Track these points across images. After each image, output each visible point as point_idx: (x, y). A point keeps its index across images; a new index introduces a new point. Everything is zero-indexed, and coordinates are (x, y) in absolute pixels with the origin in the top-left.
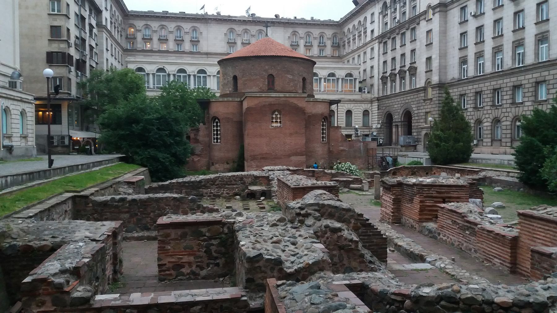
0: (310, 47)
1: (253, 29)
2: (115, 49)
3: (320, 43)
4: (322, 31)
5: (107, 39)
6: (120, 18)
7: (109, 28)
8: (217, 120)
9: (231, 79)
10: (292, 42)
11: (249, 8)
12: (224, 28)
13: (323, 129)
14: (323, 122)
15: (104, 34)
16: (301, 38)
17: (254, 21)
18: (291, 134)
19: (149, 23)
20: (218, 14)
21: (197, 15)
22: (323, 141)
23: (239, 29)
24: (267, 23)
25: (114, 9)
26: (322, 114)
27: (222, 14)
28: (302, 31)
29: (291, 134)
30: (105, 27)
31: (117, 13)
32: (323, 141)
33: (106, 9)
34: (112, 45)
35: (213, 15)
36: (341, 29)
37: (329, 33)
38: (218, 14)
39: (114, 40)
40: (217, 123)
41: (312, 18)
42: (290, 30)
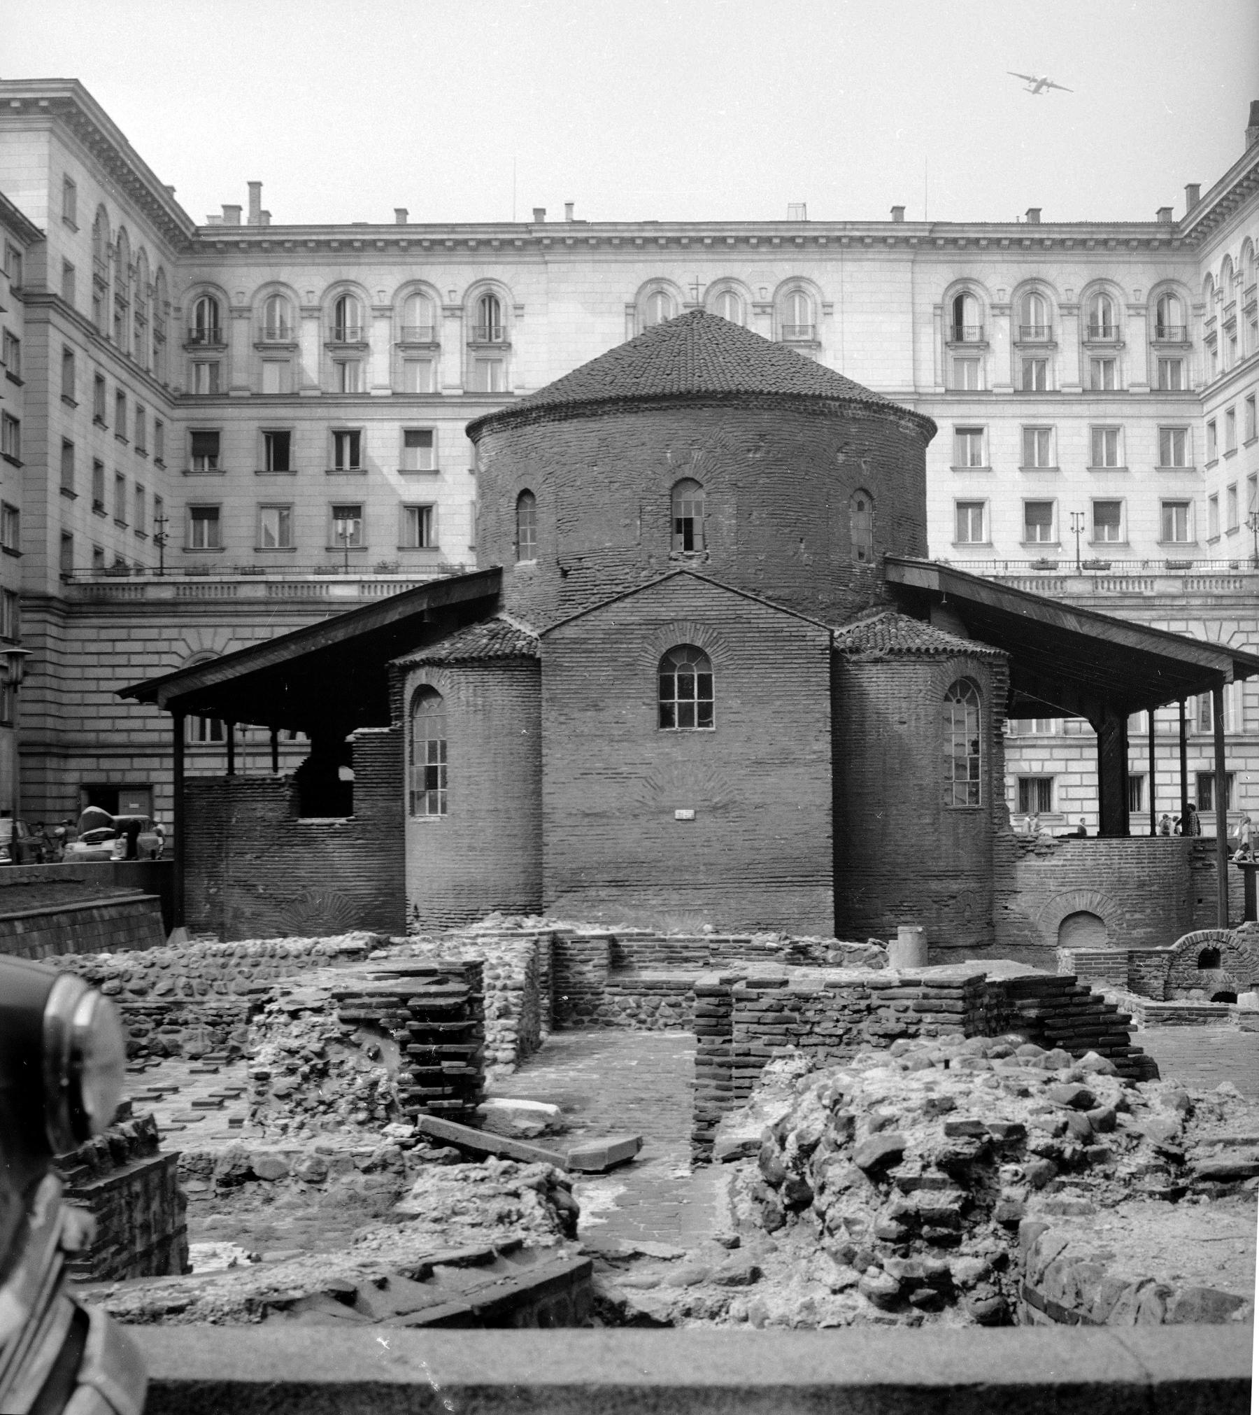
0: (1041, 353)
2: (120, 397)
4: (1099, 271)
5: (68, 355)
6: (153, 259)
7: (83, 303)
15: (51, 328)
19: (284, 274)
25: (115, 218)
30: (62, 306)
31: (136, 237)
33: (69, 221)
34: (99, 380)
36: (1198, 263)
37: (1133, 279)
39: (113, 357)
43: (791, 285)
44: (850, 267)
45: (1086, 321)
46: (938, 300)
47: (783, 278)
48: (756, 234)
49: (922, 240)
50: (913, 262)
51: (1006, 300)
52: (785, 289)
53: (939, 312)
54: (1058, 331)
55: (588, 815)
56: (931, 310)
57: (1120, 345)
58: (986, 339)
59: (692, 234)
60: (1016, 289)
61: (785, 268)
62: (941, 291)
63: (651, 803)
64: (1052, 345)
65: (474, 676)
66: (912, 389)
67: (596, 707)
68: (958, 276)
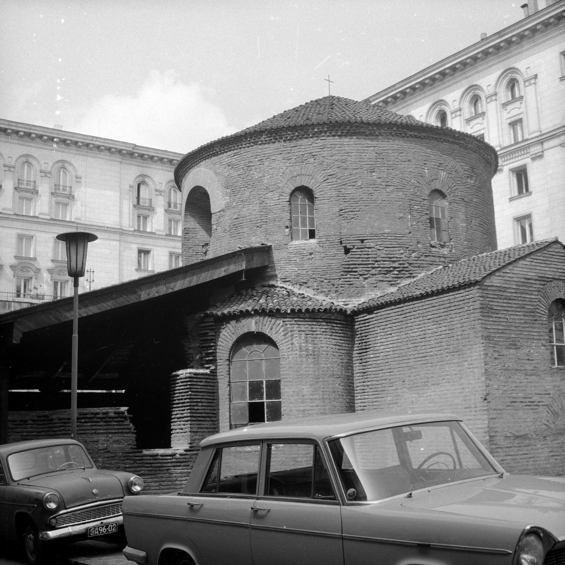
43: (60, 164)
46: (132, 183)
47: (57, 160)
48: (47, 134)
50: (121, 162)
51: (163, 188)
52: (57, 165)
53: (131, 189)
55: (517, 437)
56: (128, 188)
58: (153, 206)
59: (14, 128)
62: (133, 180)
63: (552, 426)
65: (305, 326)
66: (119, 227)
67: (514, 345)
68: (141, 173)
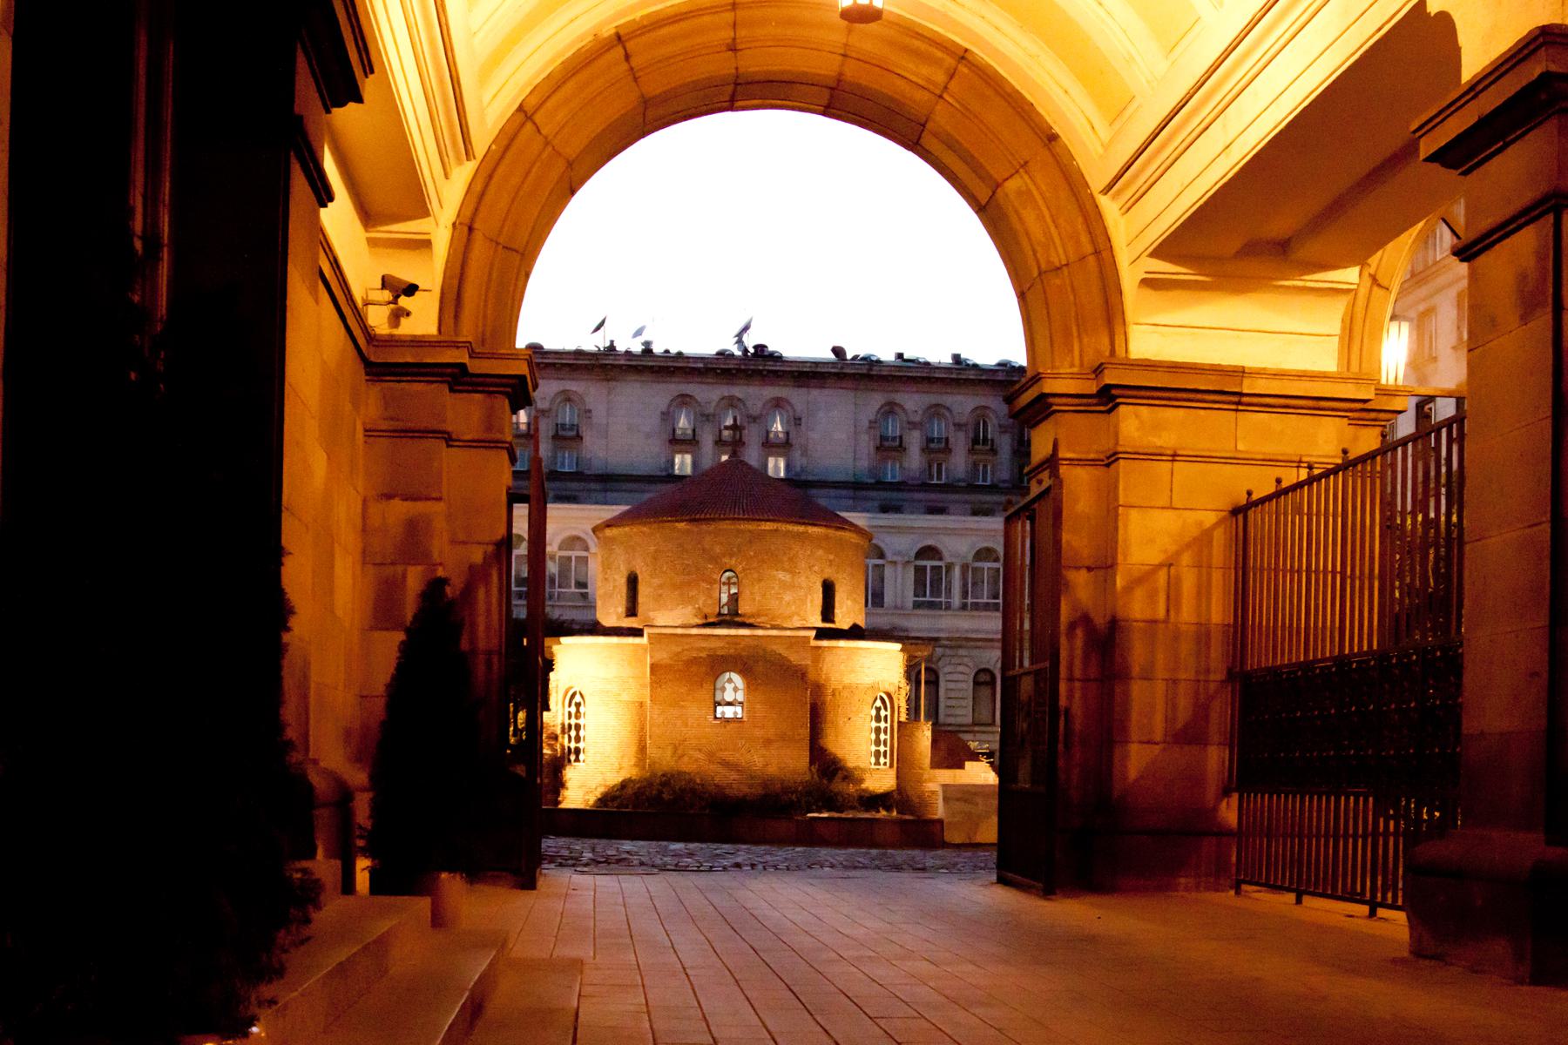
1: (756, 395)
3: (975, 441)
8: (578, 699)
9: (622, 581)
10: (883, 438)
11: (746, 328)
12: (659, 395)
13: (878, 730)
14: (878, 709)
16: (913, 425)
17: (759, 365)
18: (768, 742)
20: (648, 351)
21: (579, 353)
22: (877, 763)
23: (709, 394)
24: (808, 375)
26: (873, 687)
27: (658, 349)
28: (913, 402)
29: (768, 742)
32: (877, 763)
35: (628, 353)
38: (648, 351)
40: (578, 705)
41: (957, 358)
42: (875, 400)
44: (815, 393)
45: (971, 435)
46: (872, 417)
49: (863, 376)
54: (952, 440)
57: (993, 451)
60: (925, 412)
61: (770, 392)
64: (947, 450)
